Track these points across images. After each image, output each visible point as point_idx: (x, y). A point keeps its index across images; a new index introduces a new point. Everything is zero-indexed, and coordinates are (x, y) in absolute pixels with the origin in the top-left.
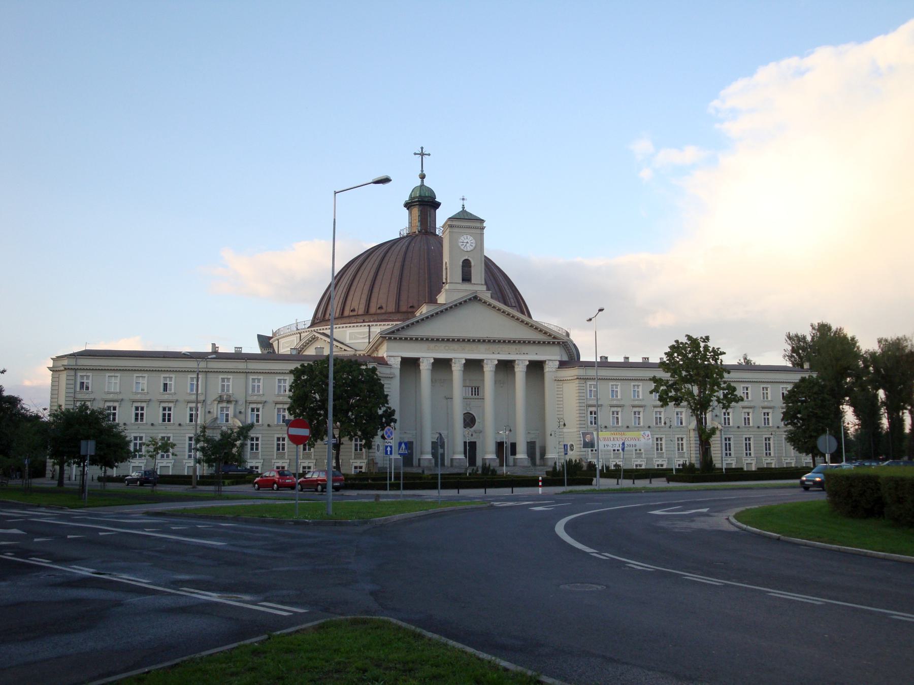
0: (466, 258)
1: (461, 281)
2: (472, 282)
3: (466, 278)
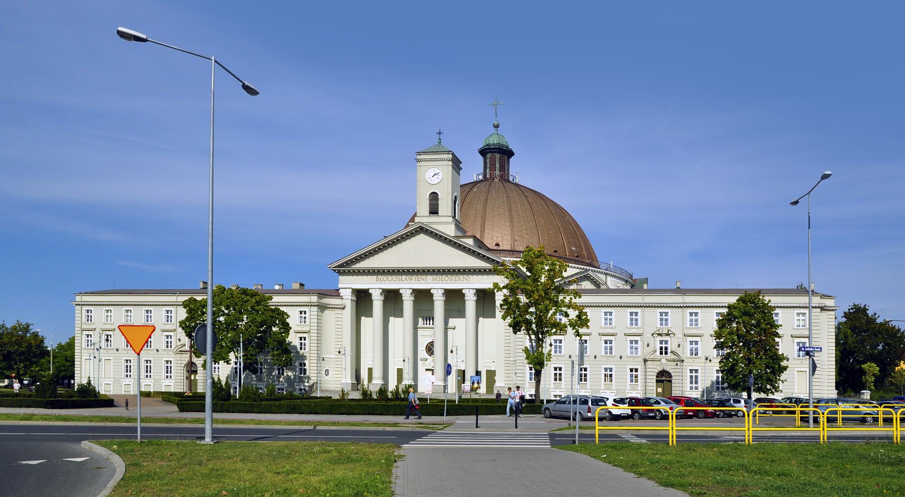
1: (428, 214)
3: (434, 211)
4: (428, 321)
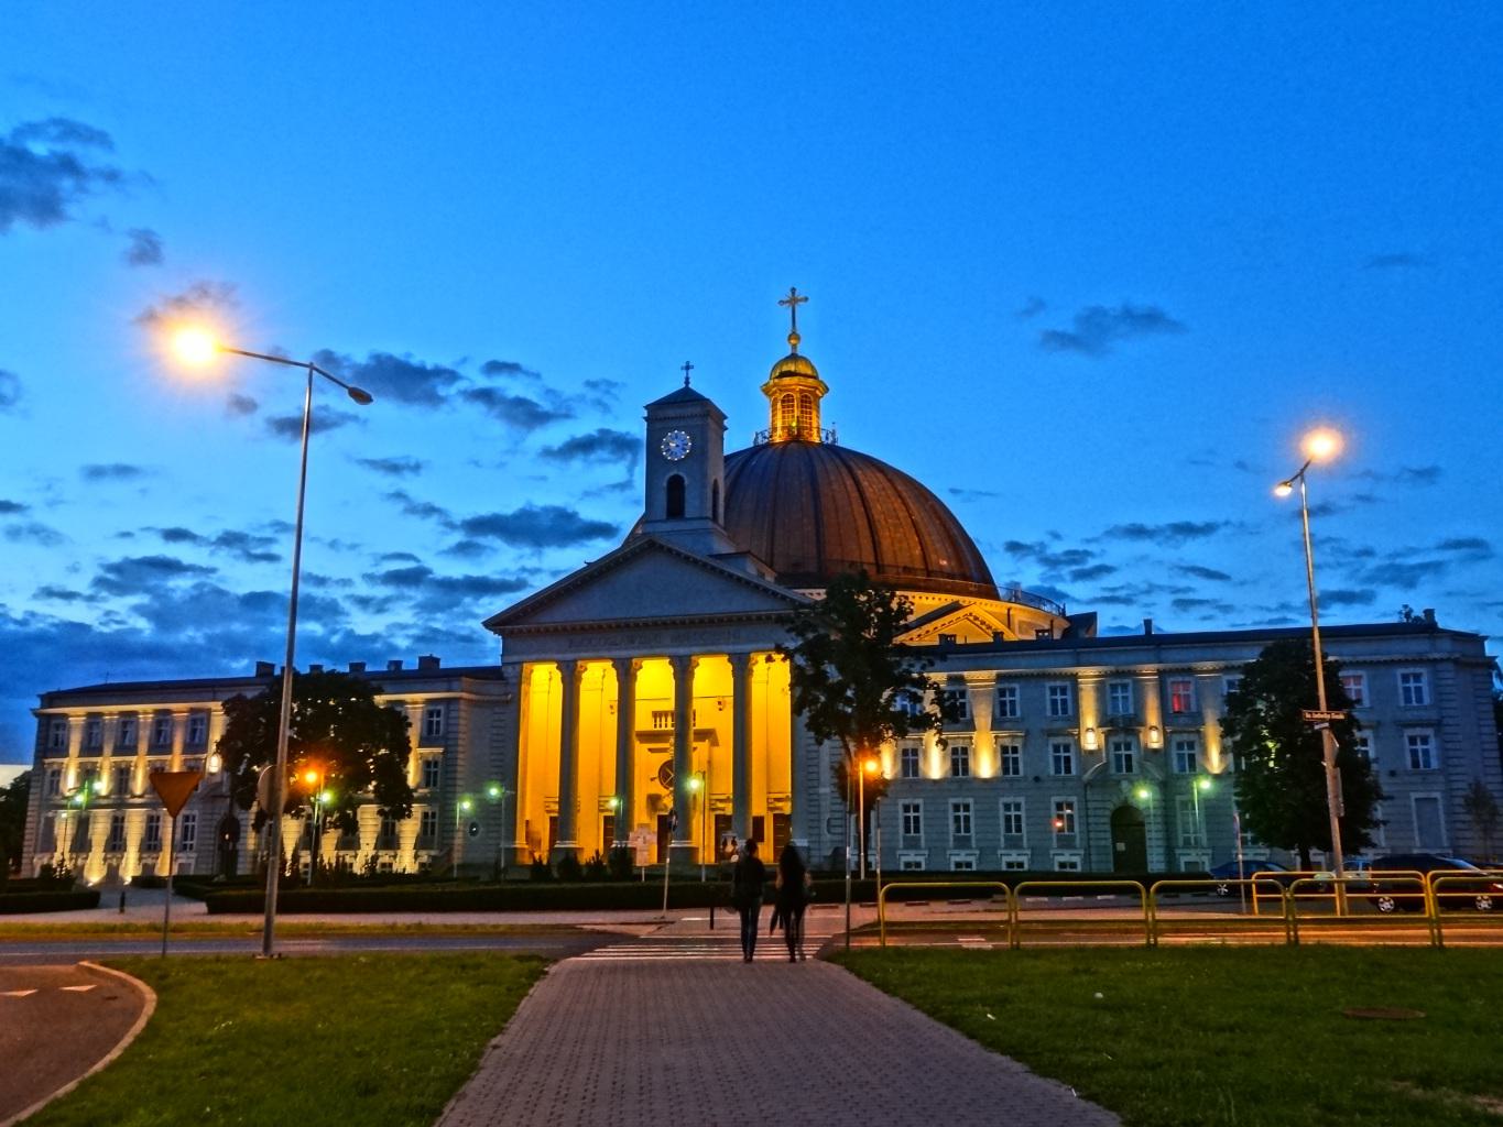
0: (672, 474)
2: (687, 516)
3: (676, 509)
4: (663, 719)
